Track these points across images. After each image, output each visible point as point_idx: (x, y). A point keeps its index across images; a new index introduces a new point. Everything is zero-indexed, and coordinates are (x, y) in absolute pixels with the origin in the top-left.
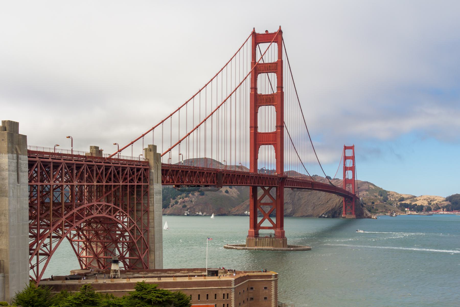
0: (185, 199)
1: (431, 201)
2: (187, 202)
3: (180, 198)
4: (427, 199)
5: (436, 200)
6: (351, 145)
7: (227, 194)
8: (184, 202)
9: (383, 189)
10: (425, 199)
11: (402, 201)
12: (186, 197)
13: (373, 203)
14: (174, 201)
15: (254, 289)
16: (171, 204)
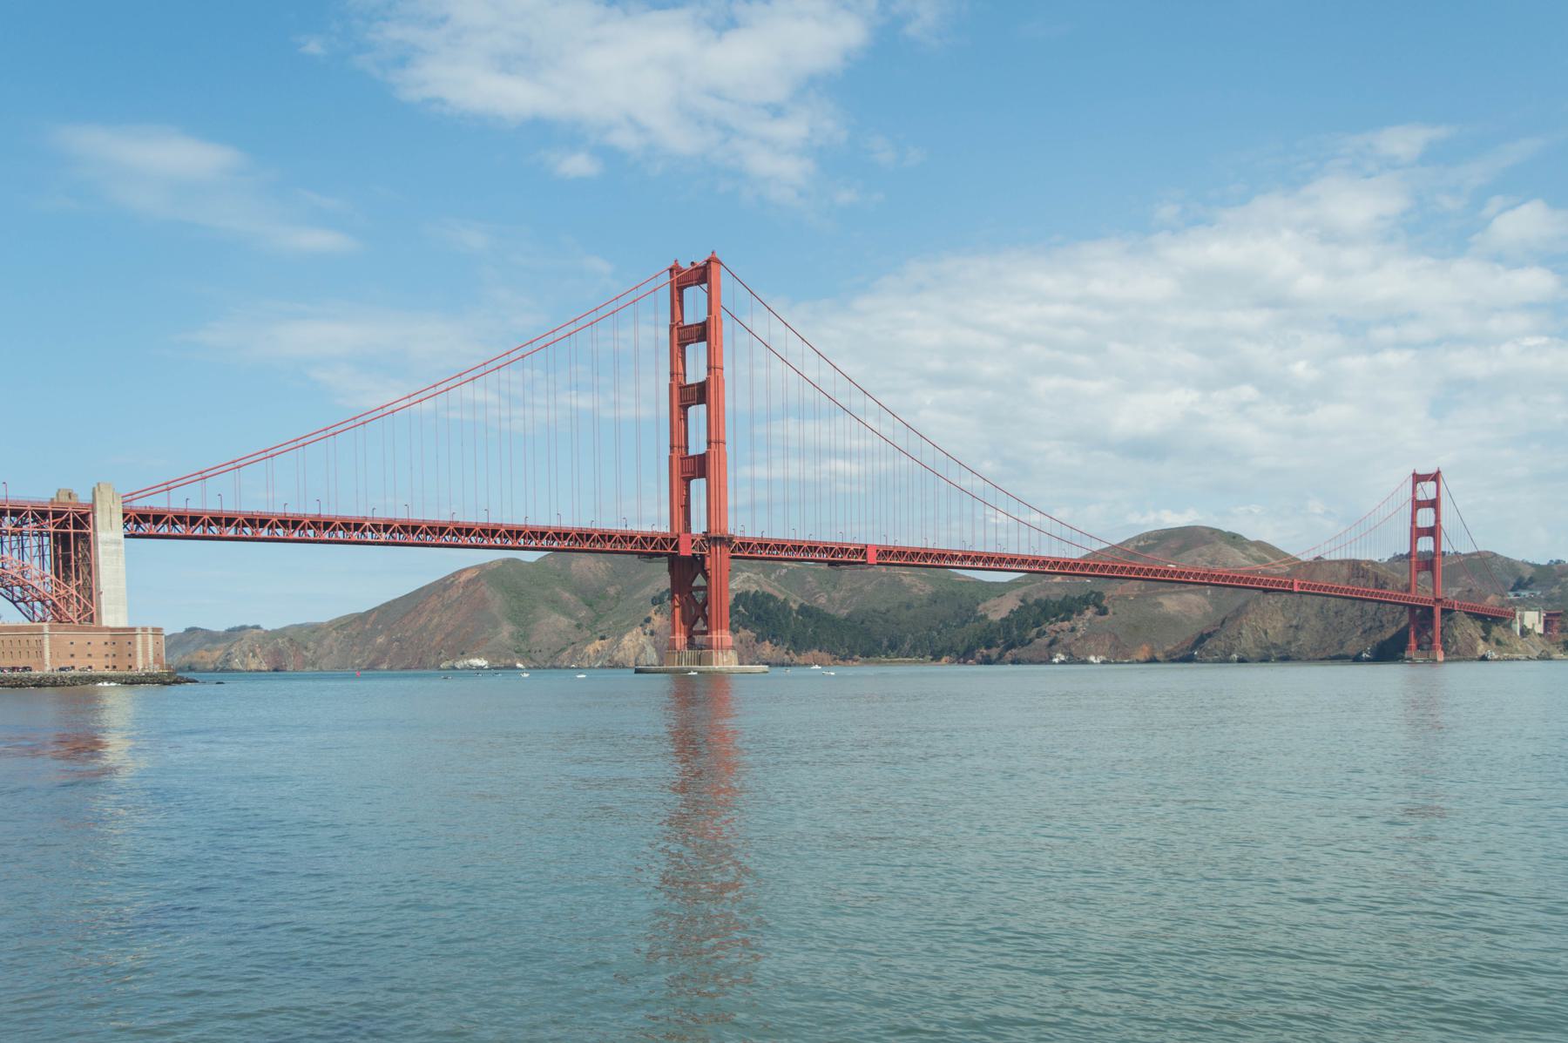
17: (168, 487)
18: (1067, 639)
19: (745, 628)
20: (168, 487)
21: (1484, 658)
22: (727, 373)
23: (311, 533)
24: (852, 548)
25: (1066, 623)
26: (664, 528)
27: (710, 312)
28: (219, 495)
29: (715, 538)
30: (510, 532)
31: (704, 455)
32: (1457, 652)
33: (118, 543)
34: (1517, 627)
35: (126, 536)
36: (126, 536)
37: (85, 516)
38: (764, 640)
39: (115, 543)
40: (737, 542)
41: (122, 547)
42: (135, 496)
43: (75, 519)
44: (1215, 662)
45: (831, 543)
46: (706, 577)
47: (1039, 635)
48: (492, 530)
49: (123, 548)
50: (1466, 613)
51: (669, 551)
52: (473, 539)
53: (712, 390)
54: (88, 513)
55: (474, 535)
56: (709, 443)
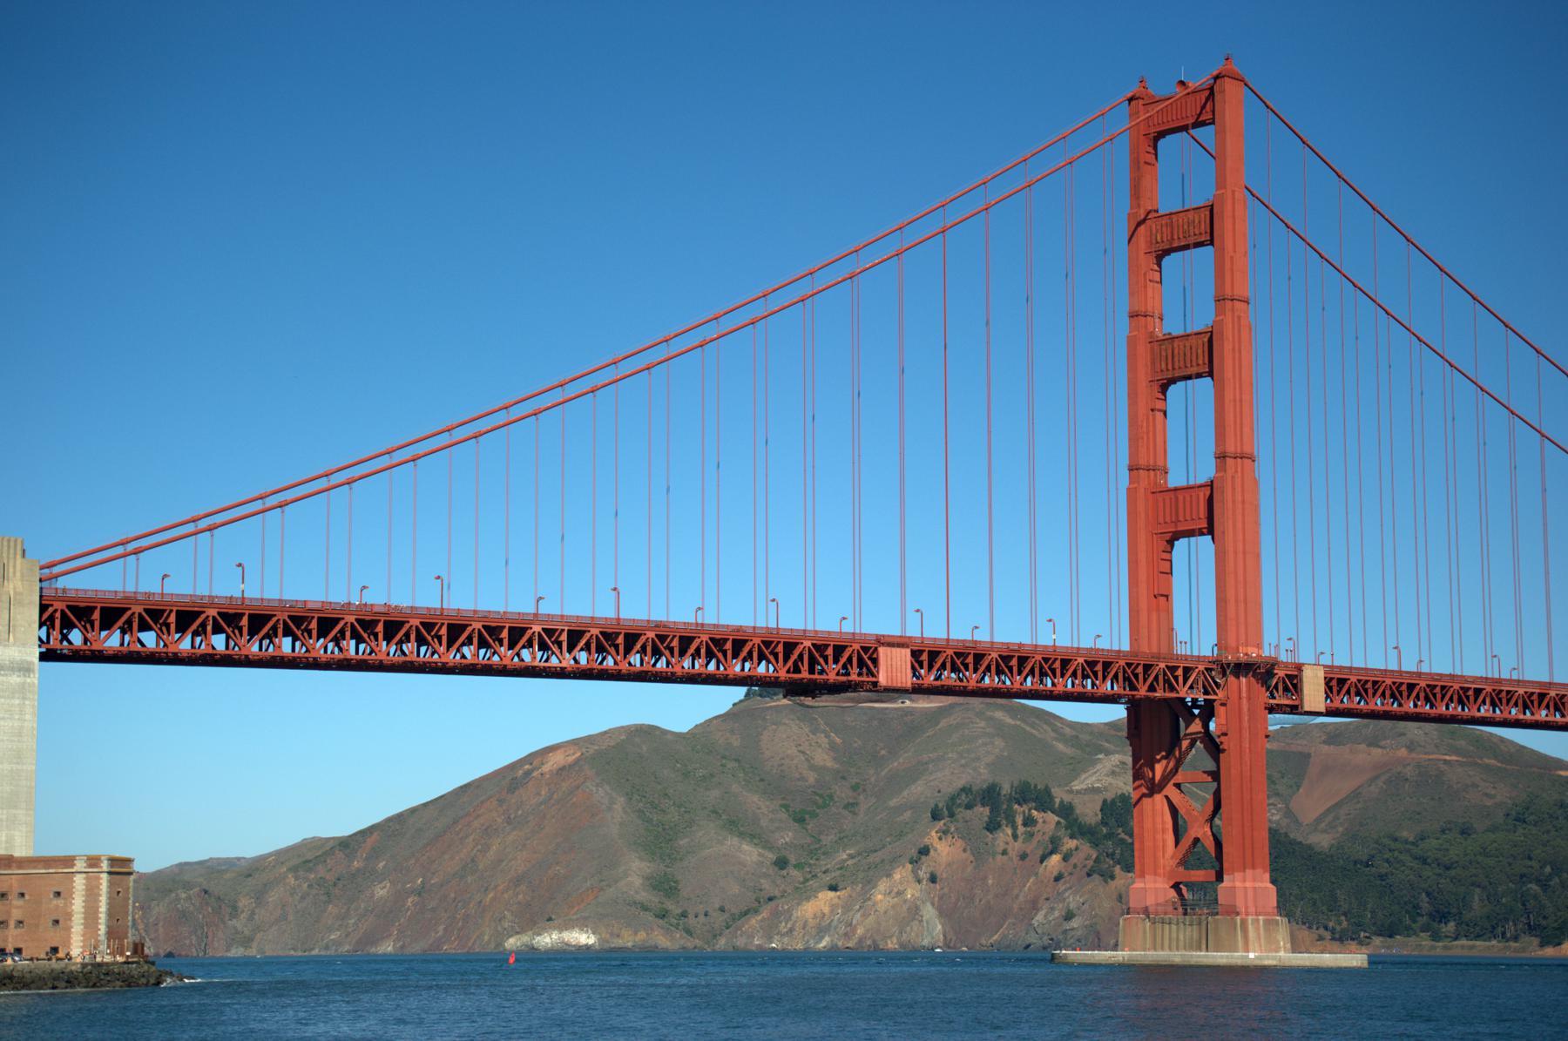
15: (27, 897)
17: (130, 548)
20: (130, 548)
23: (149, 639)
24: (1521, 691)
26: (1126, 647)
27: (1221, 183)
28: (240, 565)
30: (609, 636)
31: (1211, 484)
33: (25, 669)
35: (48, 656)
36: (48, 656)
40: (1280, 673)
41: (33, 679)
42: (56, 570)
45: (1476, 679)
46: (1214, 747)
48: (734, 641)
49: (36, 682)
51: (1143, 691)
52: (526, 654)
53: (1228, 346)
55: (529, 644)
56: (1221, 457)
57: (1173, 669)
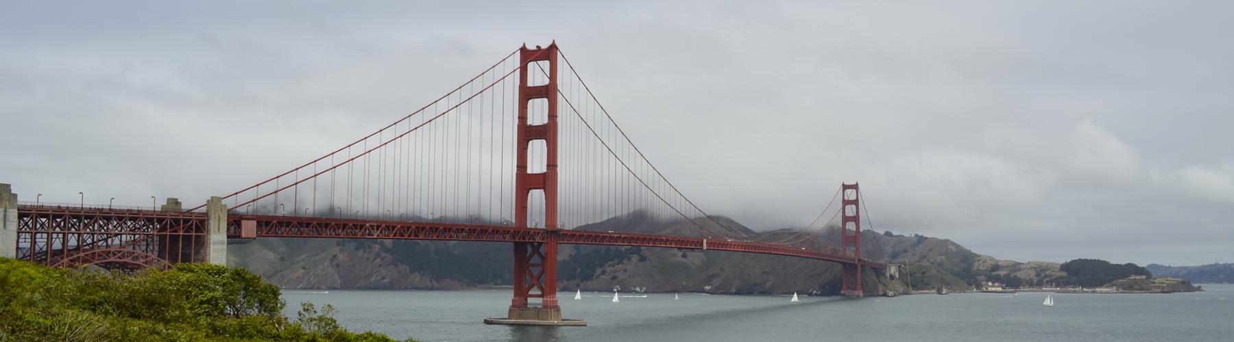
0: (616, 266)
1: (1041, 271)
2: (618, 271)
3: (610, 266)
4: (1036, 268)
5: (1050, 269)
6: (854, 183)
7: (683, 260)
8: (614, 272)
9: (973, 251)
10: (1032, 268)
11: (996, 270)
12: (618, 264)
13: (924, 273)
14: (601, 269)
16: (596, 274)
18: (621, 276)
19: (402, 263)
21: (885, 295)
22: (559, 120)
25: (620, 266)
29: (552, 231)
32: (869, 291)
34: (888, 275)
37: (202, 222)
38: (415, 272)
39: (221, 243)
43: (196, 223)
44: (721, 294)
47: (604, 272)
50: (872, 268)
54: (204, 220)
56: (548, 166)
57: (535, 232)
